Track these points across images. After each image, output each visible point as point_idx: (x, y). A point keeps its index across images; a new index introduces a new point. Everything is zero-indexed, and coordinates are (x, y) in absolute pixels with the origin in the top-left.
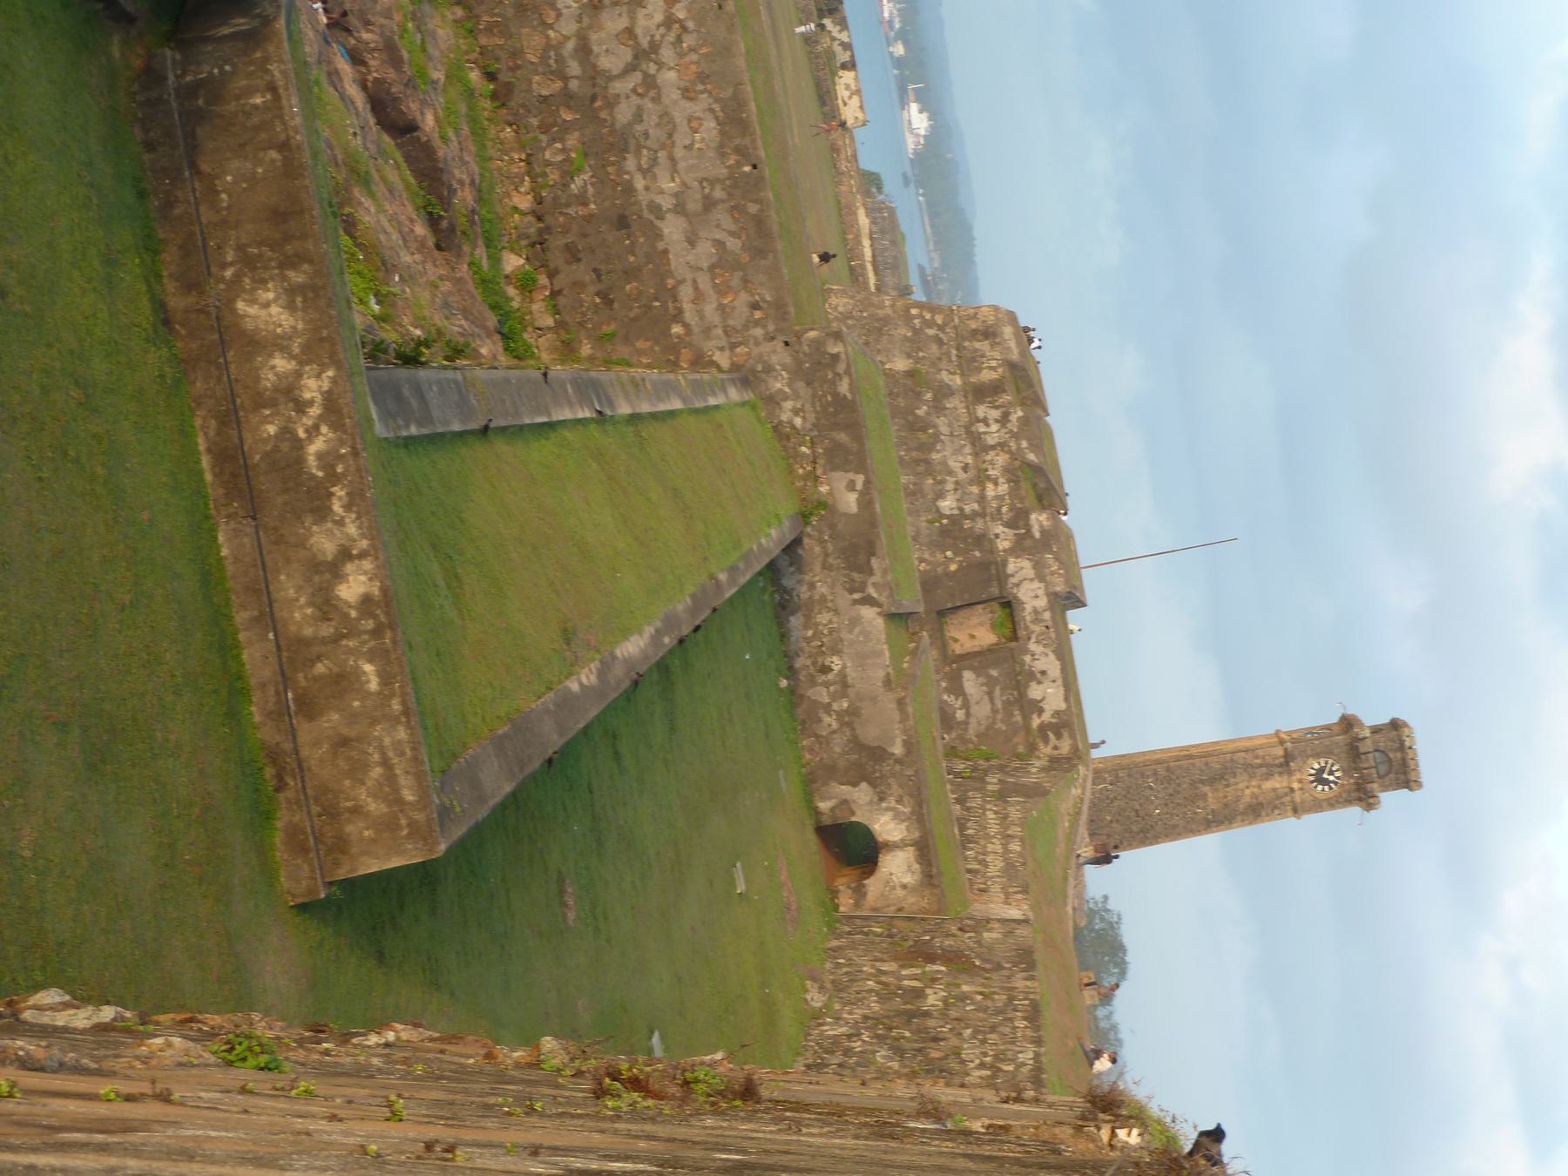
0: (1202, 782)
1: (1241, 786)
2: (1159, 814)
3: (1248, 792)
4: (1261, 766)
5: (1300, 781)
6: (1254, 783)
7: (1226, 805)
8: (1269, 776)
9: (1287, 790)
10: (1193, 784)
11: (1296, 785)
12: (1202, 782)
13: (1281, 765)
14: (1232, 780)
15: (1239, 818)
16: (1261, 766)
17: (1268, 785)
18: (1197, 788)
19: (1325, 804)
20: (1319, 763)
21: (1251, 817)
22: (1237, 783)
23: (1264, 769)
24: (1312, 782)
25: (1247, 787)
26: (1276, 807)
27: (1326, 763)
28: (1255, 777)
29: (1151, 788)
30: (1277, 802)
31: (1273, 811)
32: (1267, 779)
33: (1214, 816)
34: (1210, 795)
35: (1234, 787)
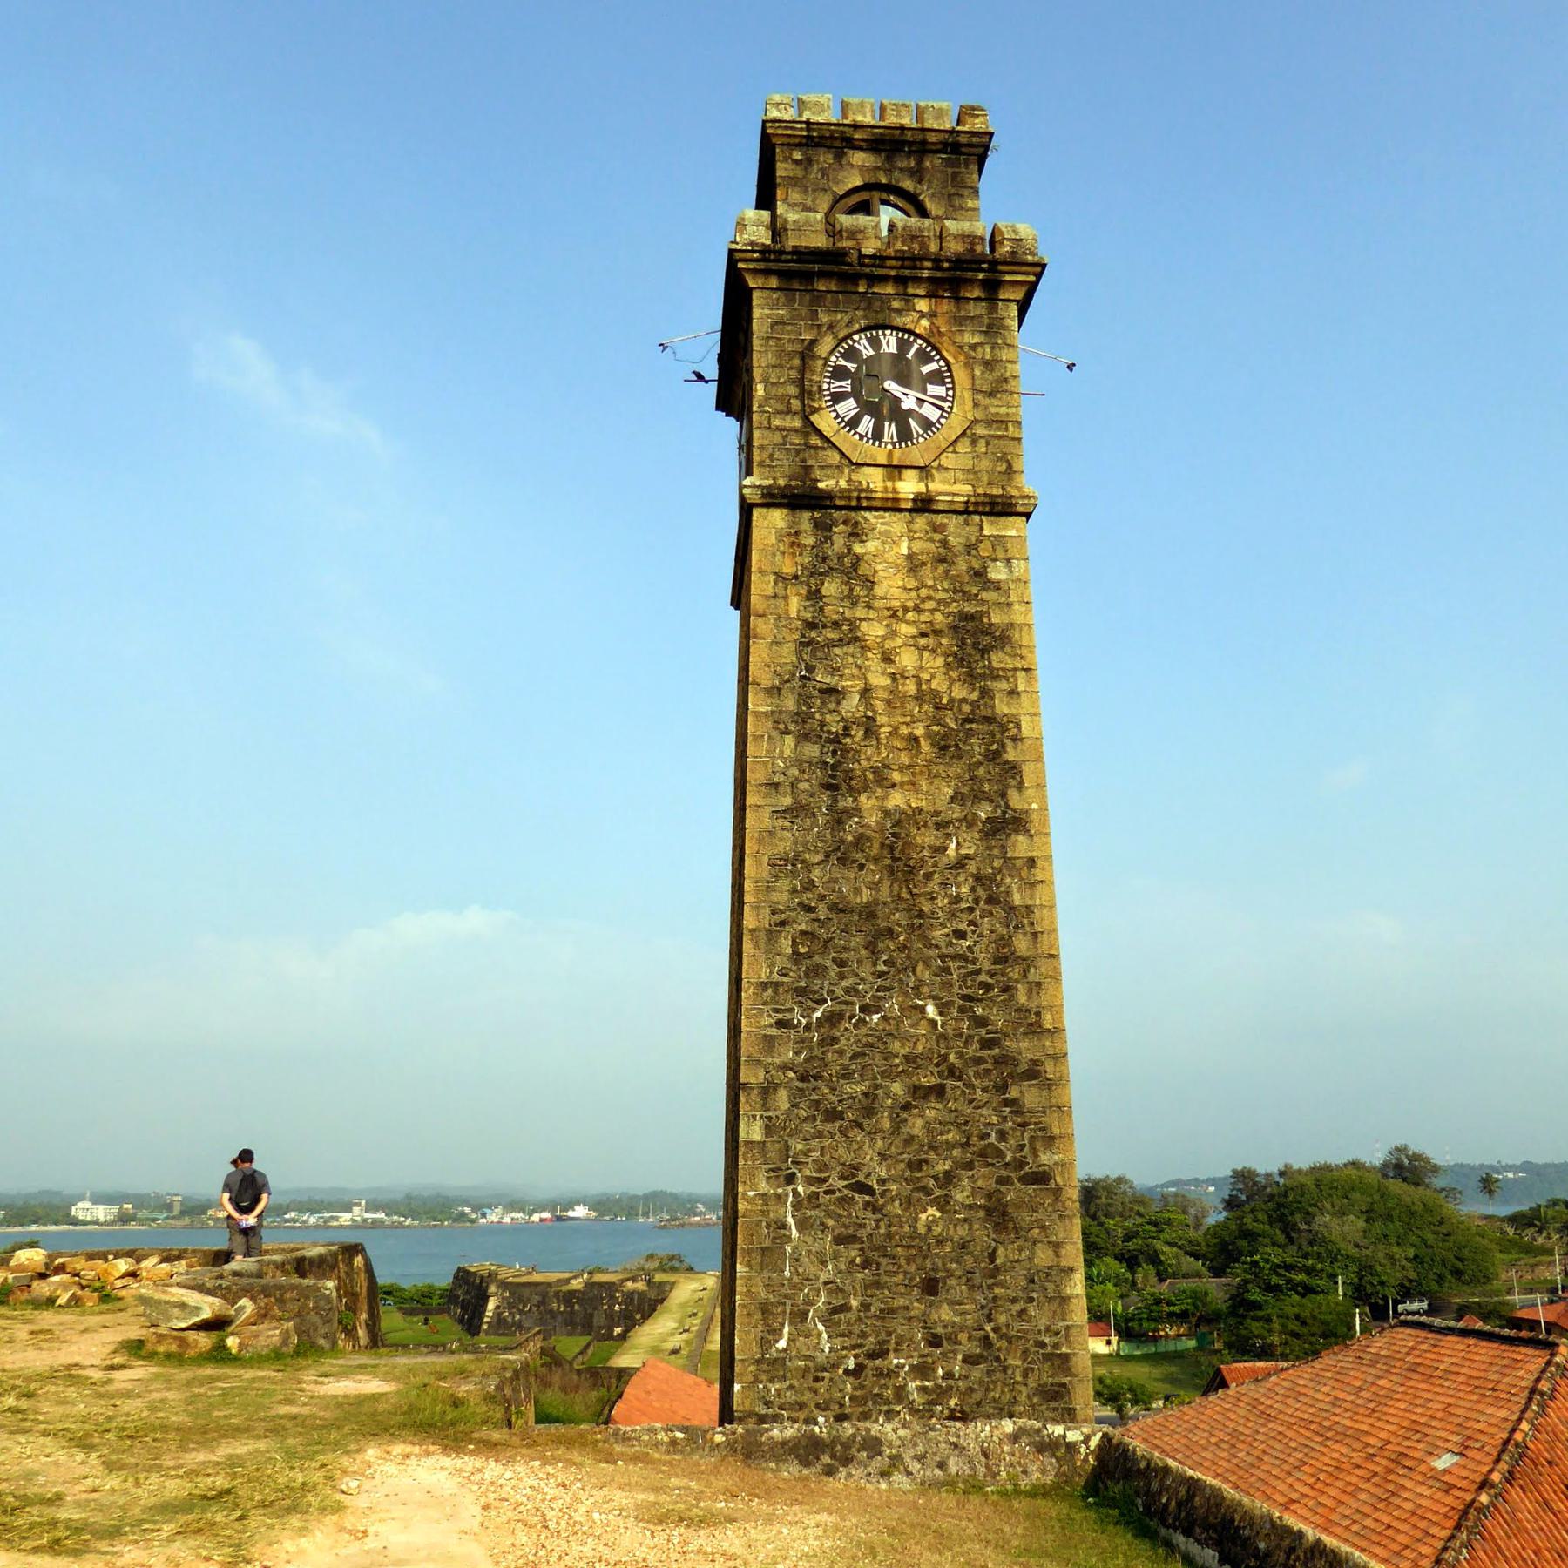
0: (838, 819)
1: (879, 680)
2: (943, 1008)
3: (907, 659)
4: (814, 595)
5: (895, 470)
6: (873, 631)
7: (945, 746)
8: (853, 571)
9: (921, 521)
10: (841, 855)
11: (909, 487)
12: (838, 819)
13: (823, 527)
14: (852, 705)
15: (1002, 707)
16: (814, 595)
17: (892, 586)
18: (860, 841)
19: (997, 408)
20: (837, 398)
21: (998, 659)
22: (866, 692)
23: (831, 588)
24: (905, 435)
25: (887, 659)
26: (980, 575)
27: (840, 373)
28: (853, 624)
29: (832, 1019)
30: (962, 565)
31: (997, 586)
32: (870, 583)
33: (978, 797)
34: (896, 800)
35: (880, 706)
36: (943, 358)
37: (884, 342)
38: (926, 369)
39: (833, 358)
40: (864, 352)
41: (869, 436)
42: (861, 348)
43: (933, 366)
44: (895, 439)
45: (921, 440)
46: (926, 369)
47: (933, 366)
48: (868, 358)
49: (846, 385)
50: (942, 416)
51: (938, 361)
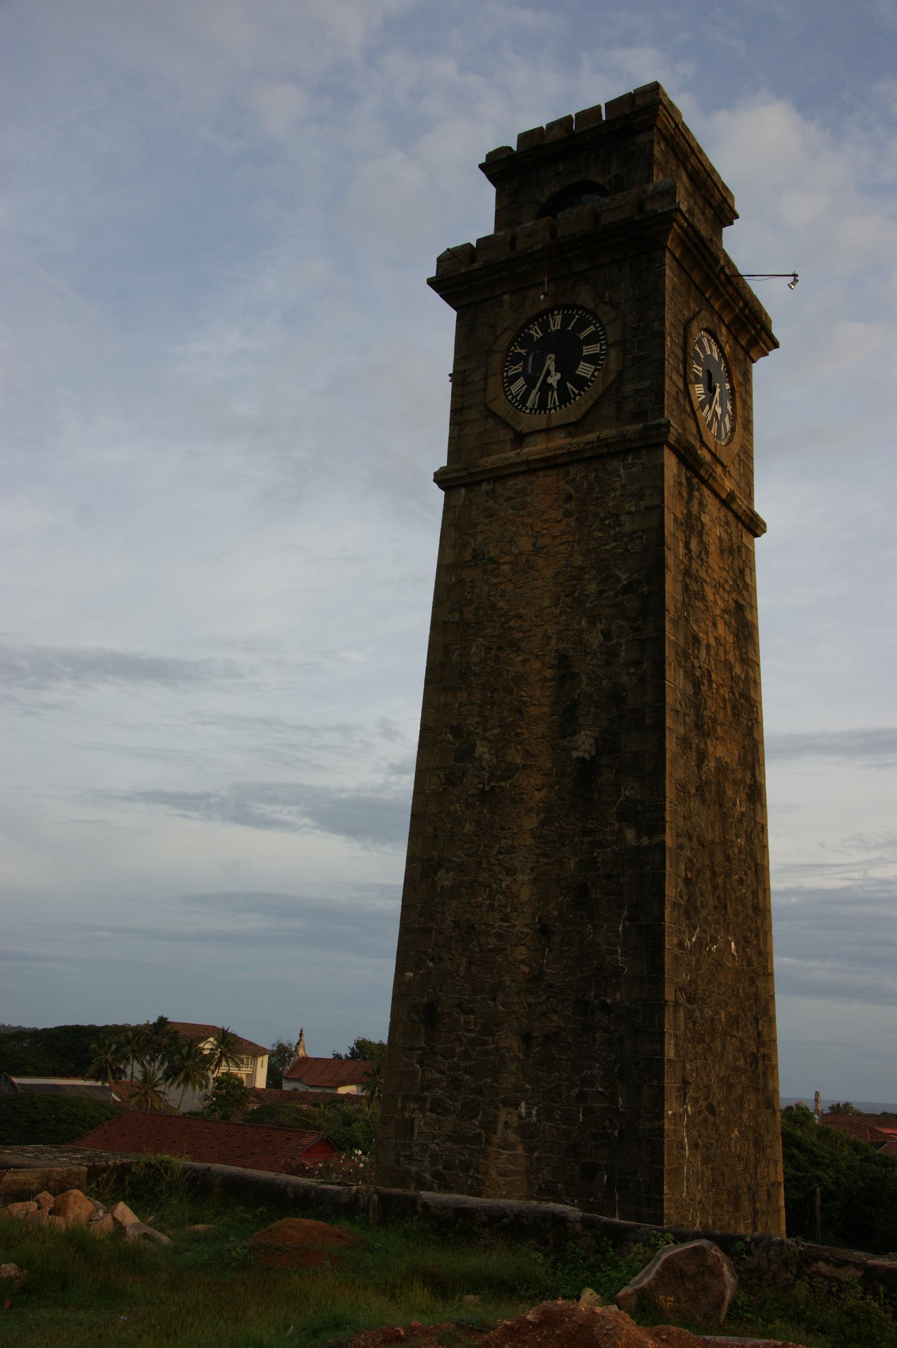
36: (599, 321)
37: (552, 323)
38: (583, 335)
39: (513, 348)
40: (535, 335)
41: (536, 407)
42: (533, 333)
43: (592, 328)
44: (557, 404)
45: (578, 398)
46: (583, 335)
47: (592, 328)
48: (538, 340)
49: (518, 368)
50: (595, 370)
51: (594, 325)
